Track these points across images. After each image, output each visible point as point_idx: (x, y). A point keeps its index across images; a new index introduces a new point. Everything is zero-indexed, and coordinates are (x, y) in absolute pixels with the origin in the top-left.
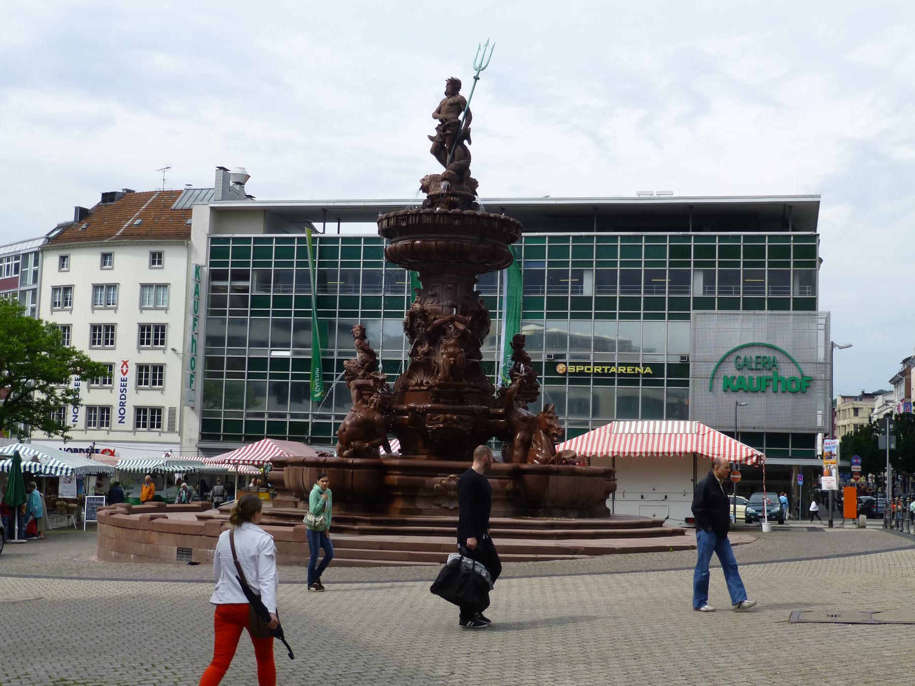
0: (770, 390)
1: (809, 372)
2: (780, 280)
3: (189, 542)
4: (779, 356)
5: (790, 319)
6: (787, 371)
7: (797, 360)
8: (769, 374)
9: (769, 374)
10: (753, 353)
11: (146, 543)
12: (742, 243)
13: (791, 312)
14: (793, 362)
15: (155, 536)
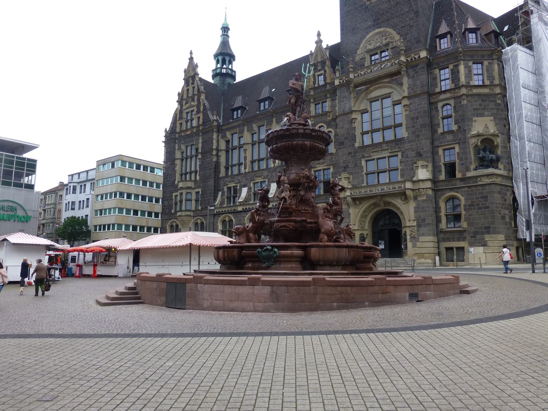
0: (12, 220)
1: (30, 214)
2: (19, 176)
3: (416, 290)
4: (18, 207)
5: (24, 191)
6: (20, 213)
7: (25, 208)
8: (13, 213)
9: (10, 213)
10: (6, 204)
11: (383, 293)
12: (4, 157)
13: (23, 189)
14: (24, 209)
15: (391, 288)
